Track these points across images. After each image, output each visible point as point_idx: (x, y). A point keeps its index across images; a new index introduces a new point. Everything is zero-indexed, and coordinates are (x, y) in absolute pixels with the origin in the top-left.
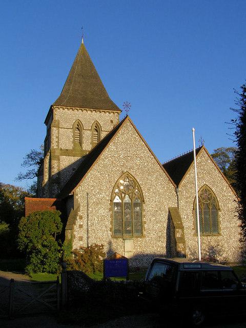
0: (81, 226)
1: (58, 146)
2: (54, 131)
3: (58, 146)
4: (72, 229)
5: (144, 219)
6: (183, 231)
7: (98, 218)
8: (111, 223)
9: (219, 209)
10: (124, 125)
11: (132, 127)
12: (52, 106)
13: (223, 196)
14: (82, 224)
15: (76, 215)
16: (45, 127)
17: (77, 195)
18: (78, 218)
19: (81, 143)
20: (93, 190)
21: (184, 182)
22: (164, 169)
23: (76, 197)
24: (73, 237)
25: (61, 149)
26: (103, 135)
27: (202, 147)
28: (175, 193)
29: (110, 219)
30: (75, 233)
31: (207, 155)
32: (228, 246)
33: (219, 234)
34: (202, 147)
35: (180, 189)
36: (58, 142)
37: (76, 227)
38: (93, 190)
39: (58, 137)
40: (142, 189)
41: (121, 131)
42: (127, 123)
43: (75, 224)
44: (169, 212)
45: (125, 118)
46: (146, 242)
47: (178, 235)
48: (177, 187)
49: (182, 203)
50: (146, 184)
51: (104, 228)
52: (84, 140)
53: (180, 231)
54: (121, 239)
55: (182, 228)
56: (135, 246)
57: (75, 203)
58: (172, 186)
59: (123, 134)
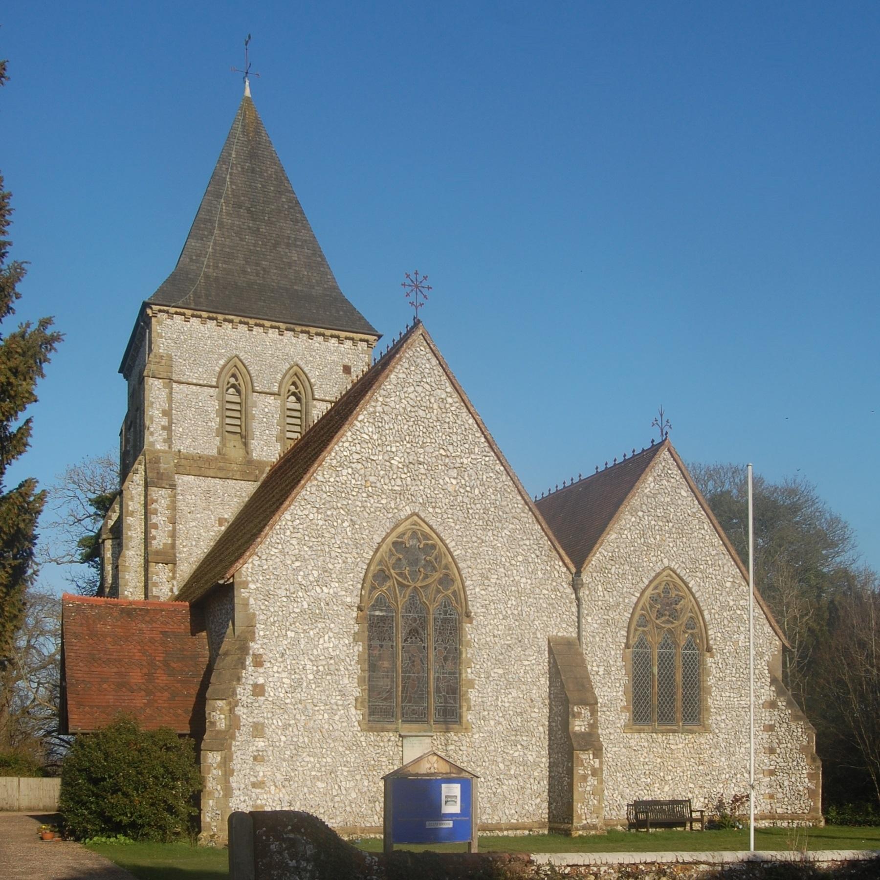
0: (258, 690)
4: (229, 695)
5: (468, 674)
7: (315, 661)
8: (361, 681)
9: (709, 650)
10: (407, 354)
11: (434, 361)
13: (722, 608)
14: (261, 681)
15: (244, 650)
17: (245, 584)
18: (249, 661)
20: (298, 569)
21: (599, 556)
22: (537, 513)
23: (241, 594)
24: (234, 723)
27: (662, 443)
28: (569, 590)
29: (356, 669)
30: (240, 711)
31: (676, 471)
32: (729, 766)
33: (706, 729)
34: (662, 443)
35: (585, 578)
37: (243, 693)
38: (298, 569)
40: (464, 573)
41: (396, 375)
43: (239, 679)
44: (550, 651)
45: (410, 331)
46: (472, 745)
47: (579, 726)
48: (578, 573)
49: (591, 623)
50: (476, 556)
53: (585, 712)
54: (393, 737)
55: (592, 704)
57: (239, 615)
58: (560, 570)
59: (402, 385)
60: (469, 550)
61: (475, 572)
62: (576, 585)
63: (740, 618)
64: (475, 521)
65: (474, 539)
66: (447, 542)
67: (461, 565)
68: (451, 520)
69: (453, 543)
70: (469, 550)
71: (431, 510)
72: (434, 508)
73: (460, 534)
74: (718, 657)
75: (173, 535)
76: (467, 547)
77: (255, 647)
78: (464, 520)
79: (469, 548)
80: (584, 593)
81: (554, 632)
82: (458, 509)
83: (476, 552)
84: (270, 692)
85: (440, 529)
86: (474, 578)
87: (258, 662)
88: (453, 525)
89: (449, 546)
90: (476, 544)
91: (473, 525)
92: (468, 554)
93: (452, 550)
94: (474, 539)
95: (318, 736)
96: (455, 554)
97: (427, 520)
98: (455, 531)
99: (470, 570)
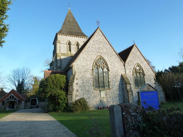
1: (60, 51)
2: (58, 45)
3: (60, 51)
6: (130, 85)
12: (57, 34)
14: (77, 82)
16: (53, 46)
18: (75, 79)
19: (70, 51)
21: (127, 61)
23: (74, 68)
25: (61, 53)
26: (80, 47)
36: (60, 50)
37: (74, 84)
39: (60, 48)
41: (96, 34)
42: (98, 31)
47: (128, 88)
49: (127, 72)
51: (89, 85)
52: (72, 49)
53: (129, 85)
55: (130, 84)
56: (106, 94)
62: (124, 66)
63: (149, 70)
67: (107, 63)
74: (146, 76)
75: (61, 64)
77: (76, 77)
80: (126, 67)
81: (122, 73)
84: (79, 84)
85: (104, 57)
87: (77, 79)
95: (87, 91)
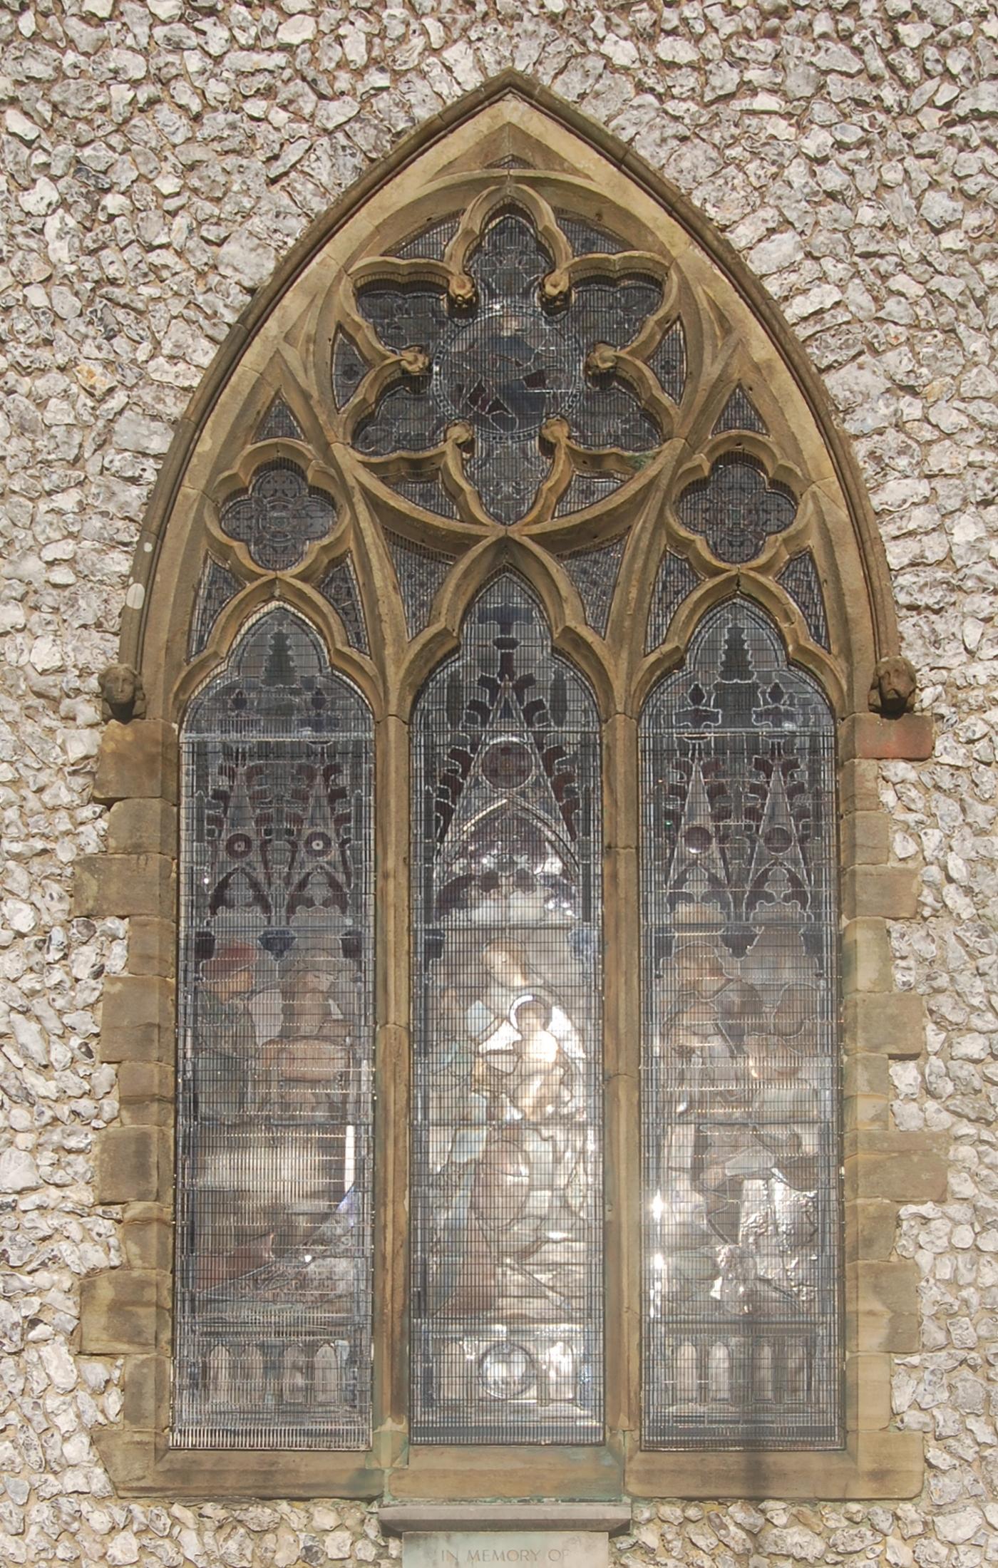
60: (900, 282)
61: (948, 417)
64: (947, 92)
65: (939, 205)
66: (741, 236)
68: (765, 101)
69: (785, 244)
70: (900, 282)
71: (623, 52)
72: (647, 37)
73: (833, 179)
76: (885, 265)
78: (864, 90)
79: (902, 267)
82: (820, 26)
83: (952, 288)
86: (941, 458)
88: (782, 129)
89: (756, 264)
90: (950, 240)
91: (931, 118)
92: (892, 305)
93: (773, 287)
94: (939, 205)
96: (796, 309)
97: (593, 112)
98: (797, 172)
99: (911, 408)
